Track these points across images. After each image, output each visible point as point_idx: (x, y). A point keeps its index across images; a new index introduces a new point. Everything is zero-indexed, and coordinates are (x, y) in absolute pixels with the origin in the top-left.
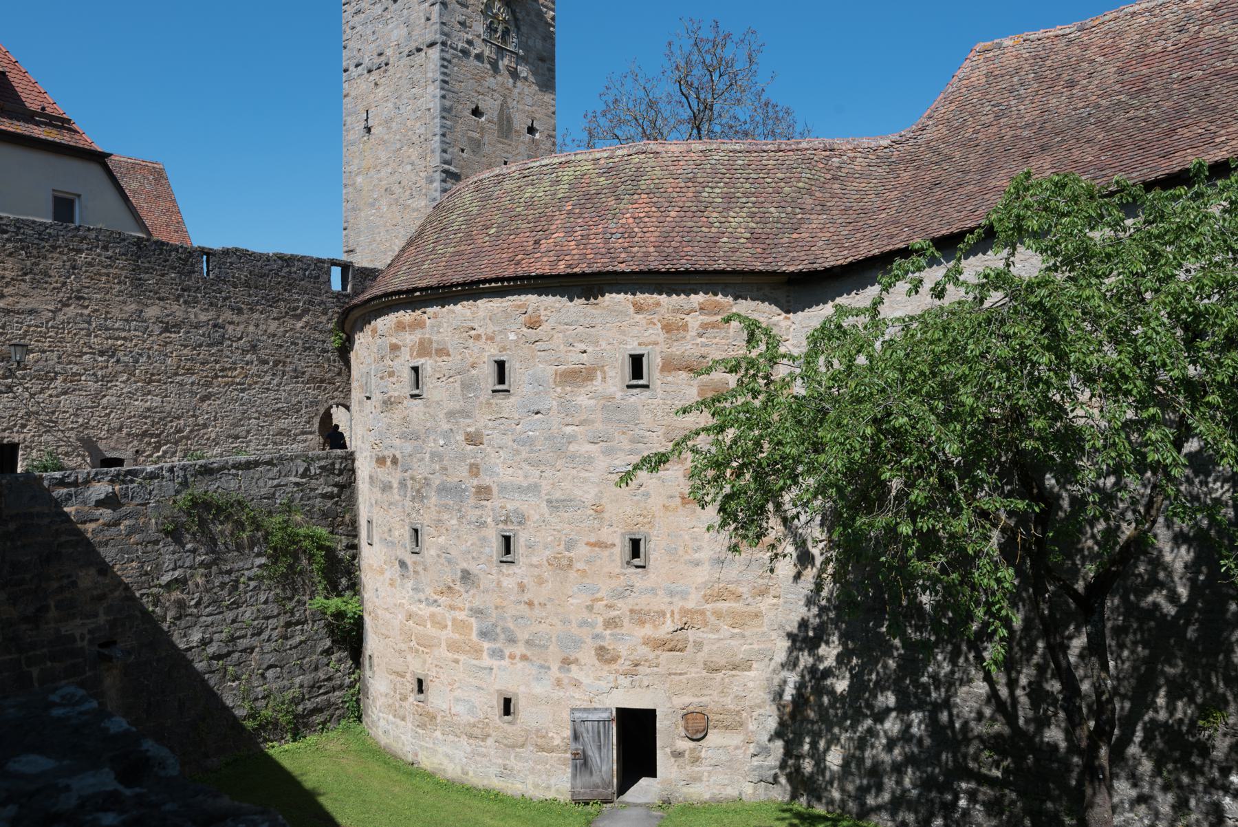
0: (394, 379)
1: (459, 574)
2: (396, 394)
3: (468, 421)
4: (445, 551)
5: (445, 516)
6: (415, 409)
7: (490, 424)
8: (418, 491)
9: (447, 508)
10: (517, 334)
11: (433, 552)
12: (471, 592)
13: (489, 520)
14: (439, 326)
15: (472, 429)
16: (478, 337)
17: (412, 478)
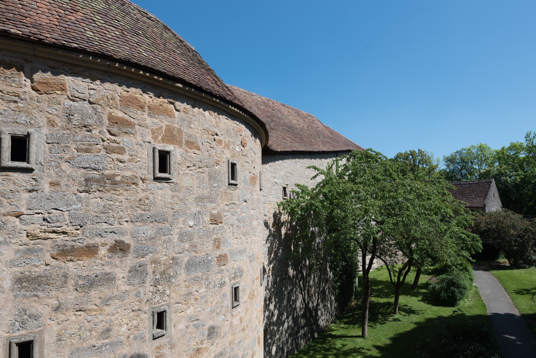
0: (125, 157)
1: (206, 333)
2: (128, 174)
3: (213, 205)
4: (194, 319)
5: (196, 288)
6: (160, 192)
7: (226, 208)
8: (163, 273)
9: (196, 280)
10: (239, 148)
11: (181, 326)
12: (217, 341)
13: (227, 280)
14: (190, 122)
15: (215, 212)
16: (220, 142)
17: (155, 262)
